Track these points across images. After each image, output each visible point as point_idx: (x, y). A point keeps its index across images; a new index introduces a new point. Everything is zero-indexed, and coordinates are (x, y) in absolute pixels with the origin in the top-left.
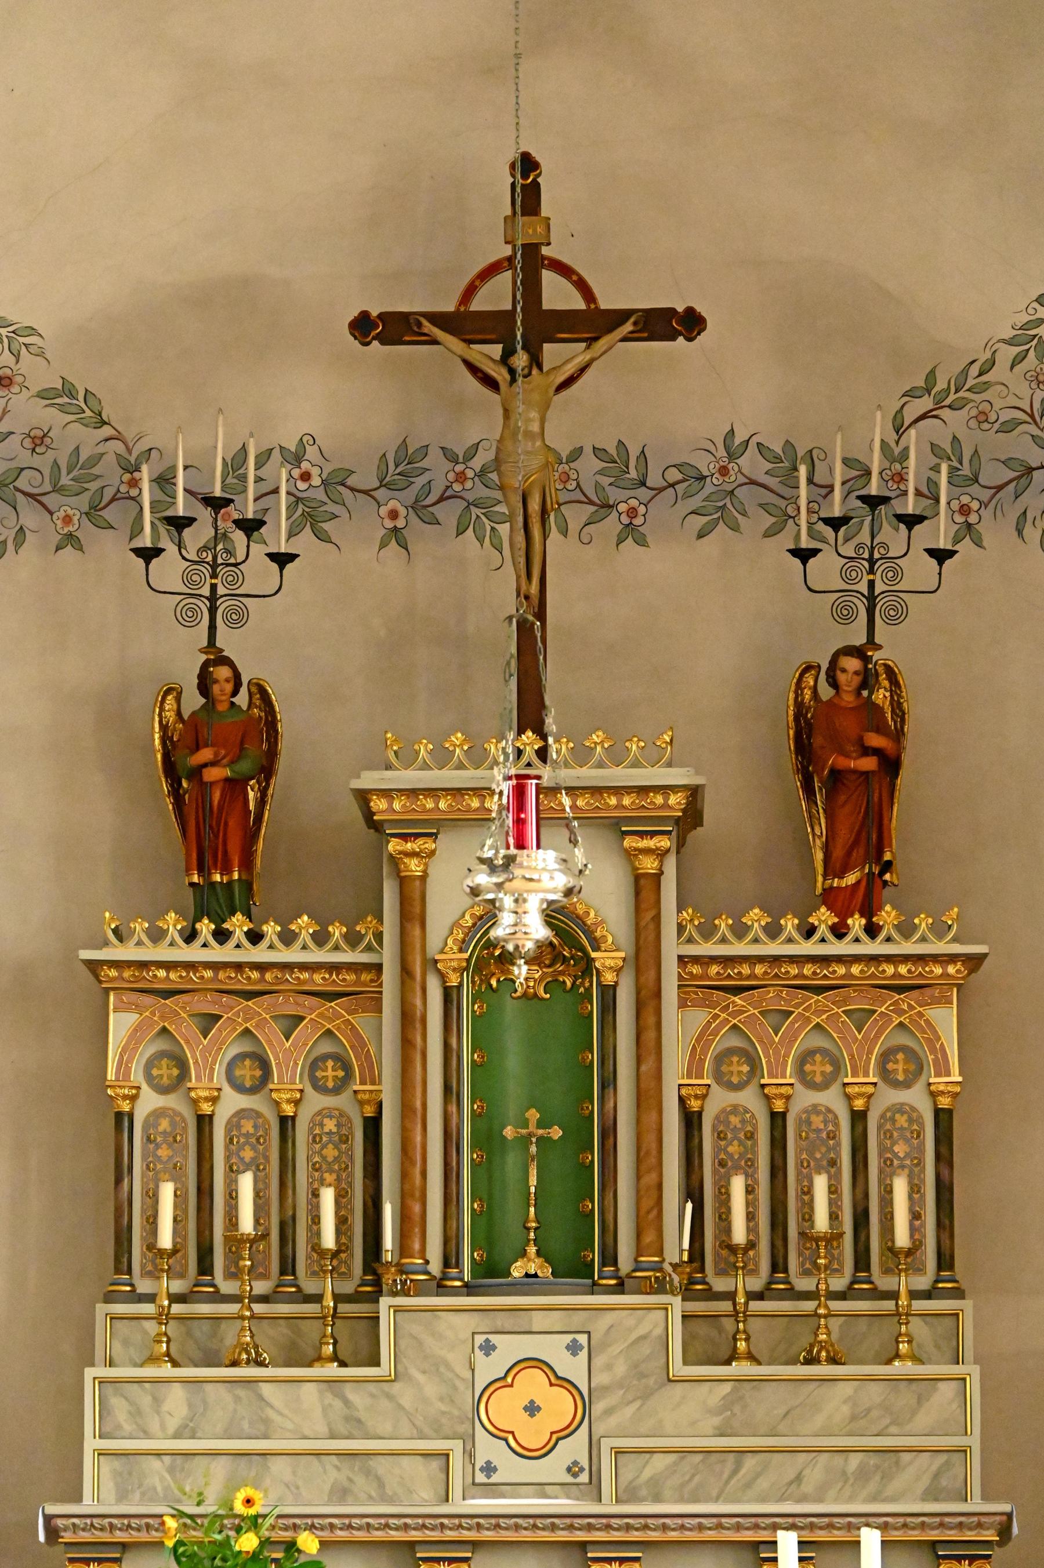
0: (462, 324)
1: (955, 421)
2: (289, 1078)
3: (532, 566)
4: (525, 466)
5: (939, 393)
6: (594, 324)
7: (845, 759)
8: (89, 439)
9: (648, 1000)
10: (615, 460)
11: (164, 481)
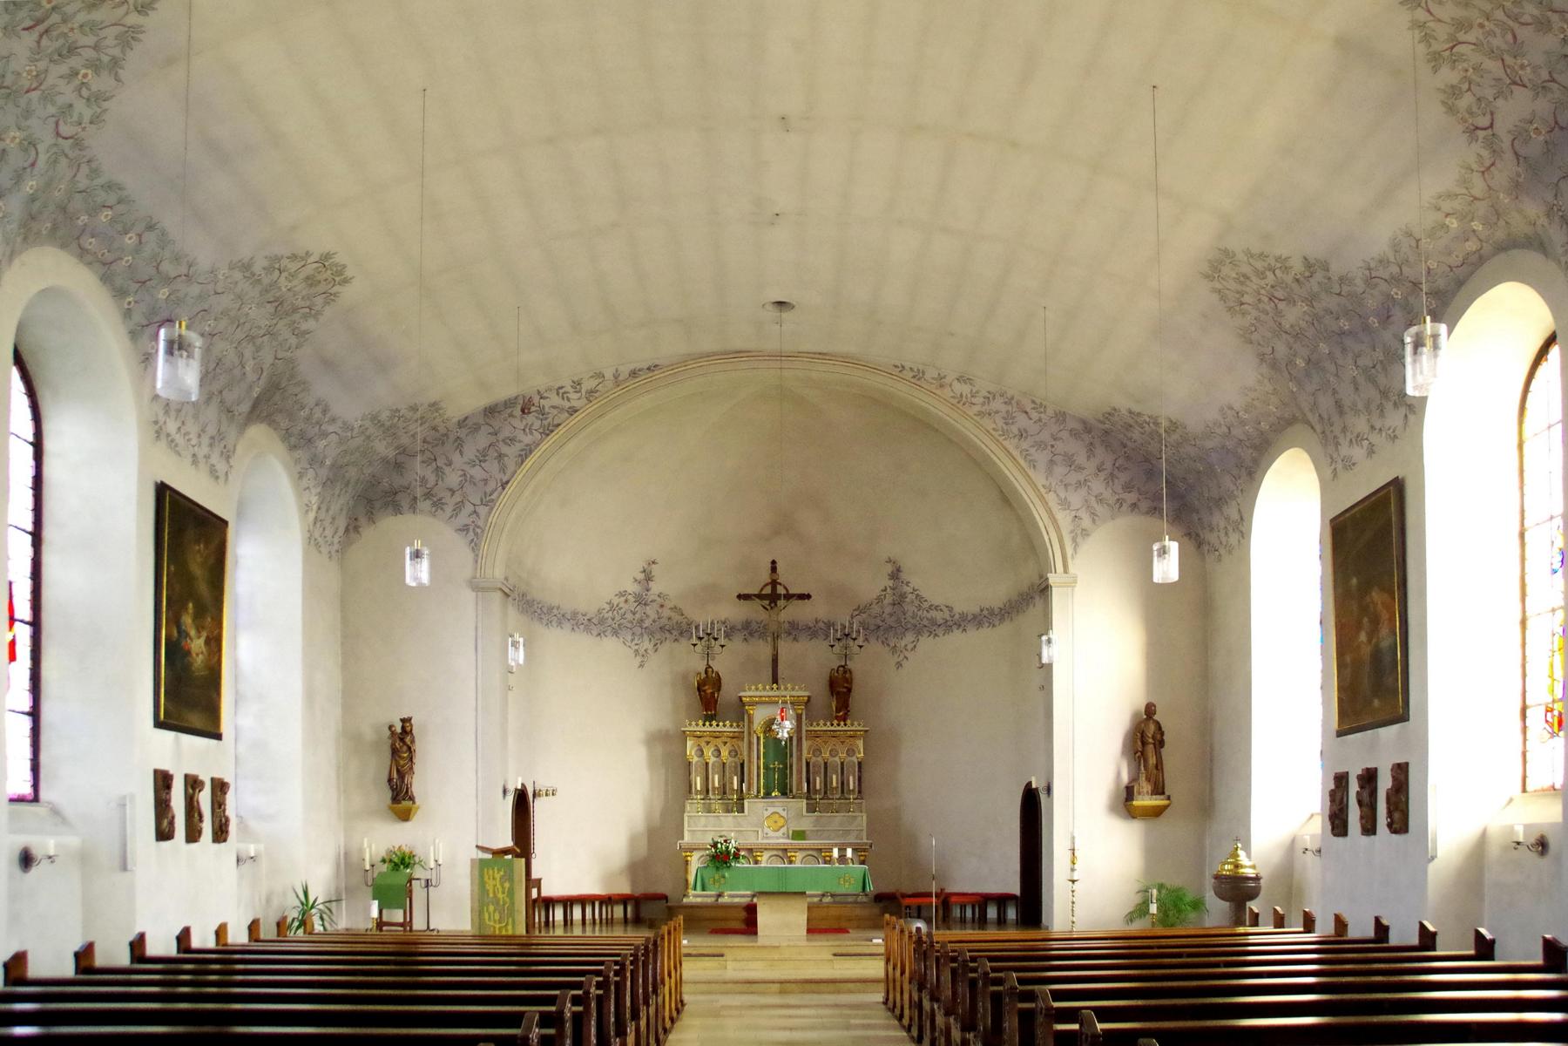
0: (760, 596)
2: (725, 753)
3: (775, 648)
4: (773, 627)
5: (860, 610)
6: (788, 597)
7: (841, 688)
9: (800, 740)
11: (697, 628)
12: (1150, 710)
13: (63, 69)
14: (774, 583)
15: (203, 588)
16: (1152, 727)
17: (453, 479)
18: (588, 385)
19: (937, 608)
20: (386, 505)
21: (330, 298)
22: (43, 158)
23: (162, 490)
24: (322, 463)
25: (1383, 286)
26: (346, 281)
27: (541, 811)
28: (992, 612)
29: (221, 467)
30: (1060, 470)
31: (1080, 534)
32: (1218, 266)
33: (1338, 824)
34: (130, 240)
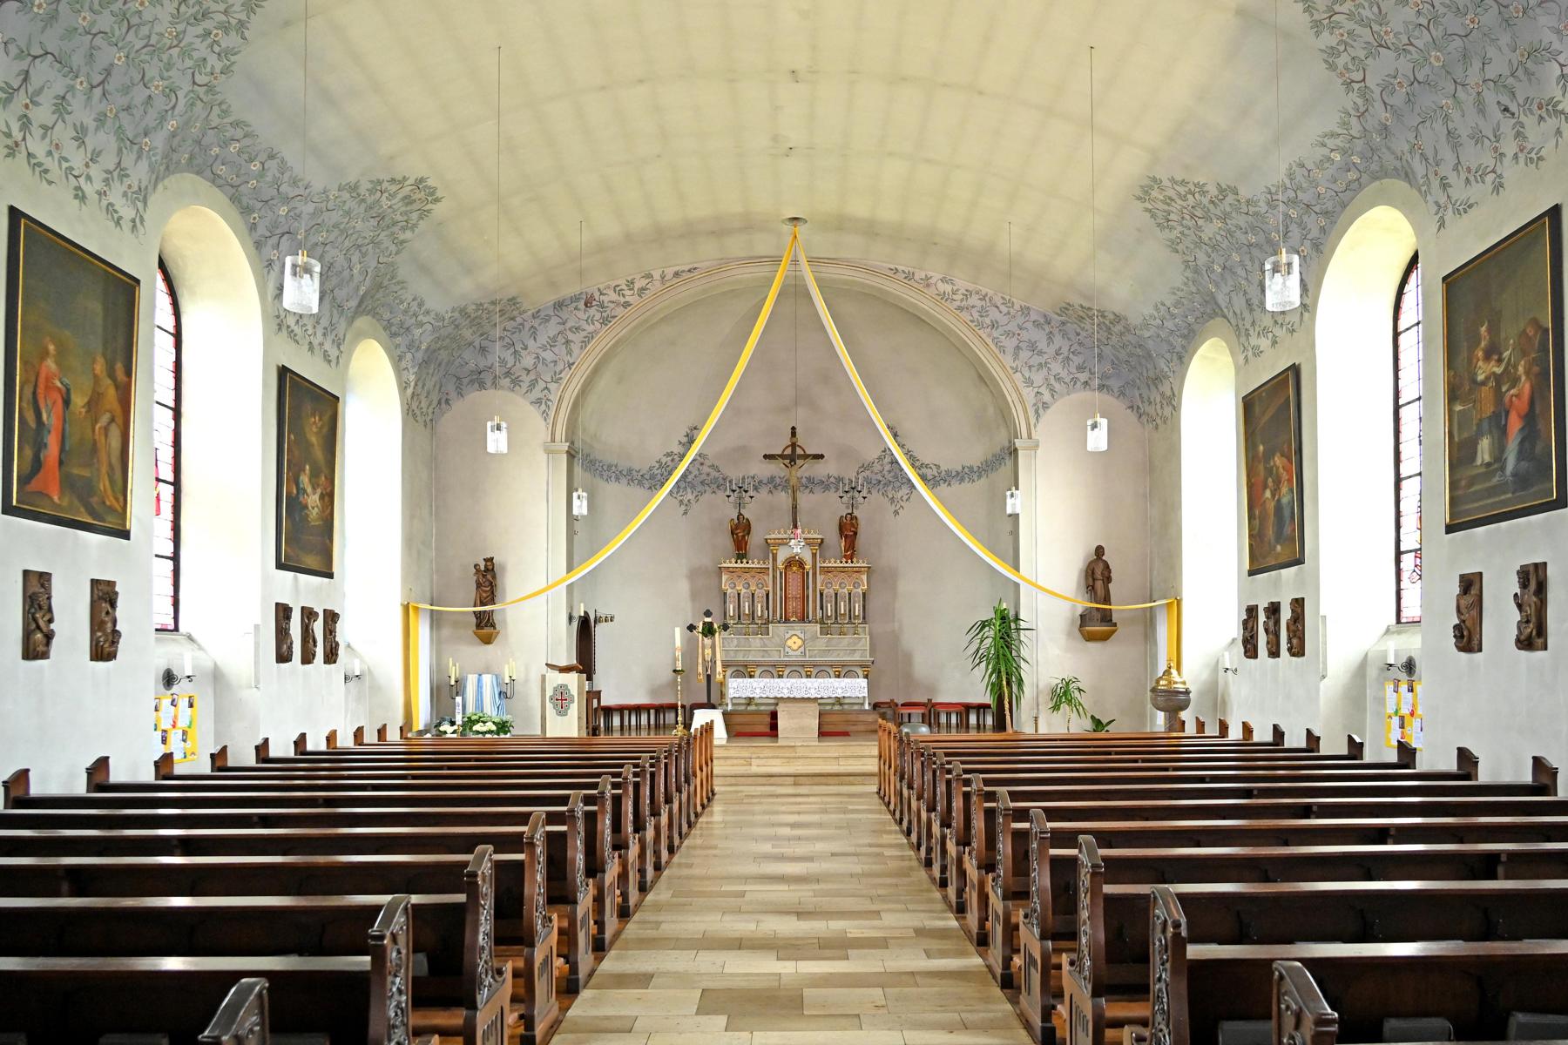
3: (794, 499)
4: (794, 481)
5: (865, 467)
6: (806, 456)
9: (814, 574)
10: (809, 479)
12: (1099, 551)
13: (199, 30)
14: (794, 445)
15: (319, 454)
16: (1101, 565)
17: (528, 361)
18: (637, 286)
20: (472, 381)
21: (424, 213)
22: (182, 102)
23: (283, 372)
24: (419, 348)
25: (1282, 207)
26: (437, 200)
27: (600, 633)
28: (971, 468)
29: (333, 352)
30: (1025, 354)
32: (1147, 190)
33: (1251, 650)
34: (255, 167)
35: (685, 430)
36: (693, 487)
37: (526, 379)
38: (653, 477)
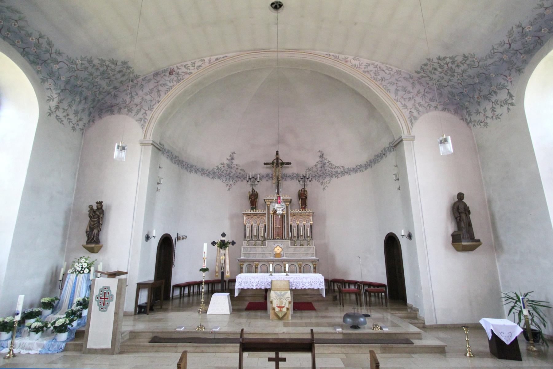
1: (310, 172)
5: (309, 170)
8: (244, 173)
9: (288, 216)
14: (277, 159)
19: (338, 167)
24: (59, 78)
28: (361, 166)
30: (401, 93)
31: (413, 119)
35: (230, 153)
36: (233, 179)
37: (135, 109)
38: (214, 173)
